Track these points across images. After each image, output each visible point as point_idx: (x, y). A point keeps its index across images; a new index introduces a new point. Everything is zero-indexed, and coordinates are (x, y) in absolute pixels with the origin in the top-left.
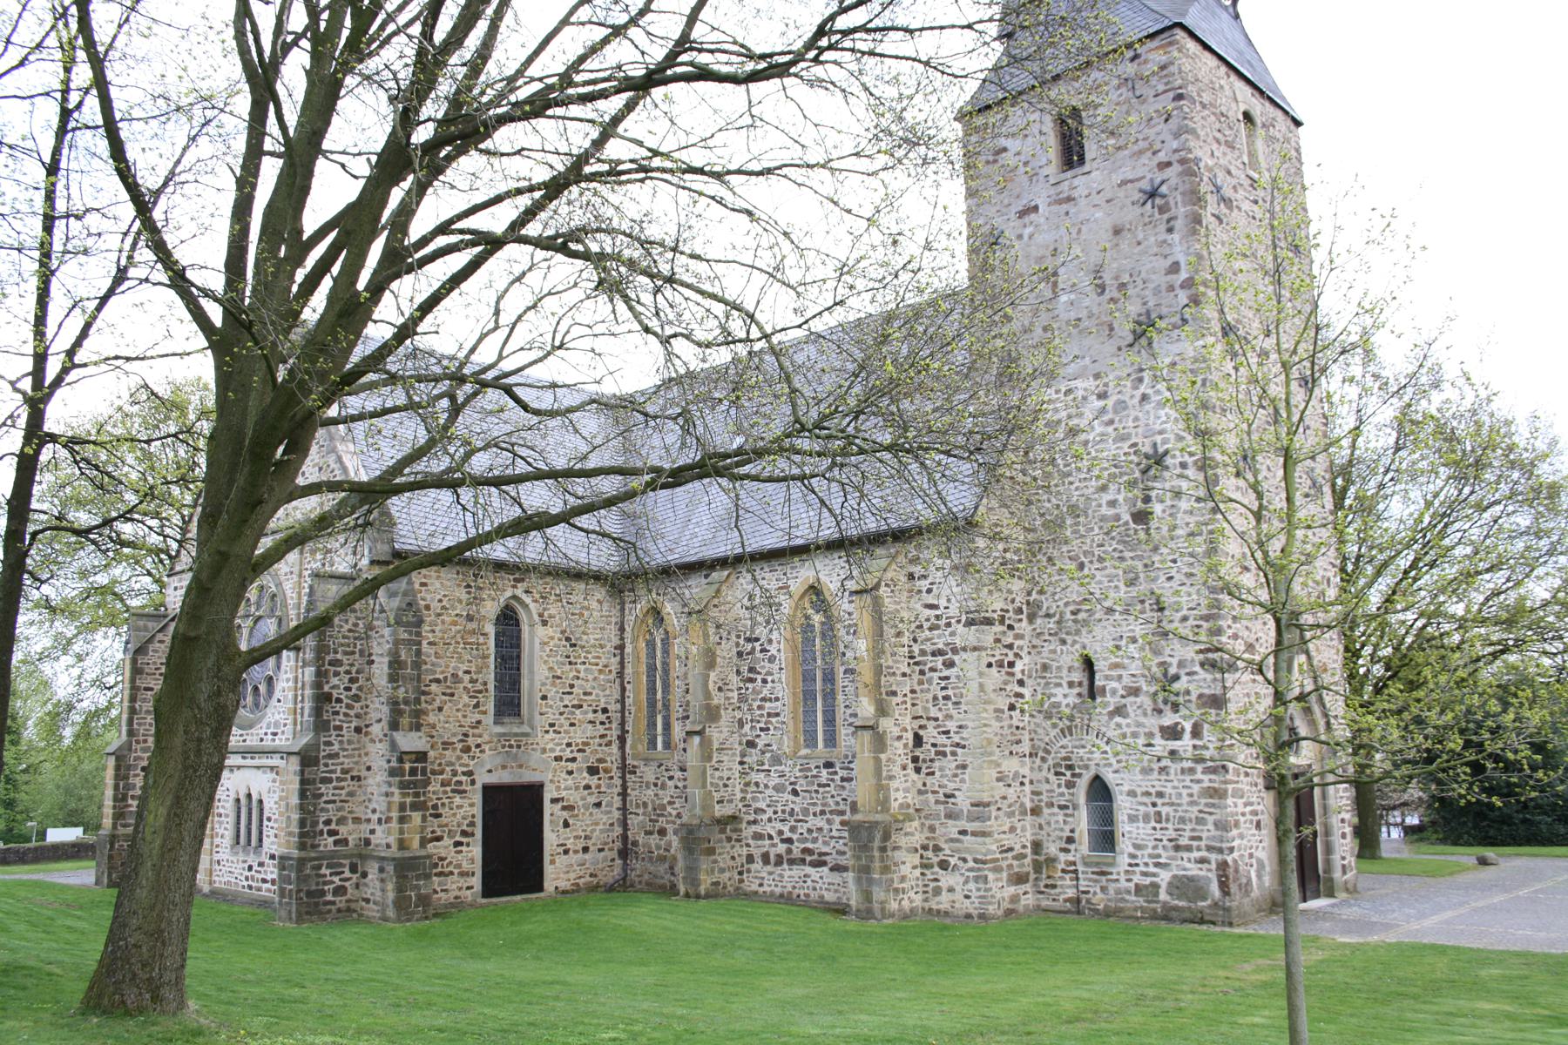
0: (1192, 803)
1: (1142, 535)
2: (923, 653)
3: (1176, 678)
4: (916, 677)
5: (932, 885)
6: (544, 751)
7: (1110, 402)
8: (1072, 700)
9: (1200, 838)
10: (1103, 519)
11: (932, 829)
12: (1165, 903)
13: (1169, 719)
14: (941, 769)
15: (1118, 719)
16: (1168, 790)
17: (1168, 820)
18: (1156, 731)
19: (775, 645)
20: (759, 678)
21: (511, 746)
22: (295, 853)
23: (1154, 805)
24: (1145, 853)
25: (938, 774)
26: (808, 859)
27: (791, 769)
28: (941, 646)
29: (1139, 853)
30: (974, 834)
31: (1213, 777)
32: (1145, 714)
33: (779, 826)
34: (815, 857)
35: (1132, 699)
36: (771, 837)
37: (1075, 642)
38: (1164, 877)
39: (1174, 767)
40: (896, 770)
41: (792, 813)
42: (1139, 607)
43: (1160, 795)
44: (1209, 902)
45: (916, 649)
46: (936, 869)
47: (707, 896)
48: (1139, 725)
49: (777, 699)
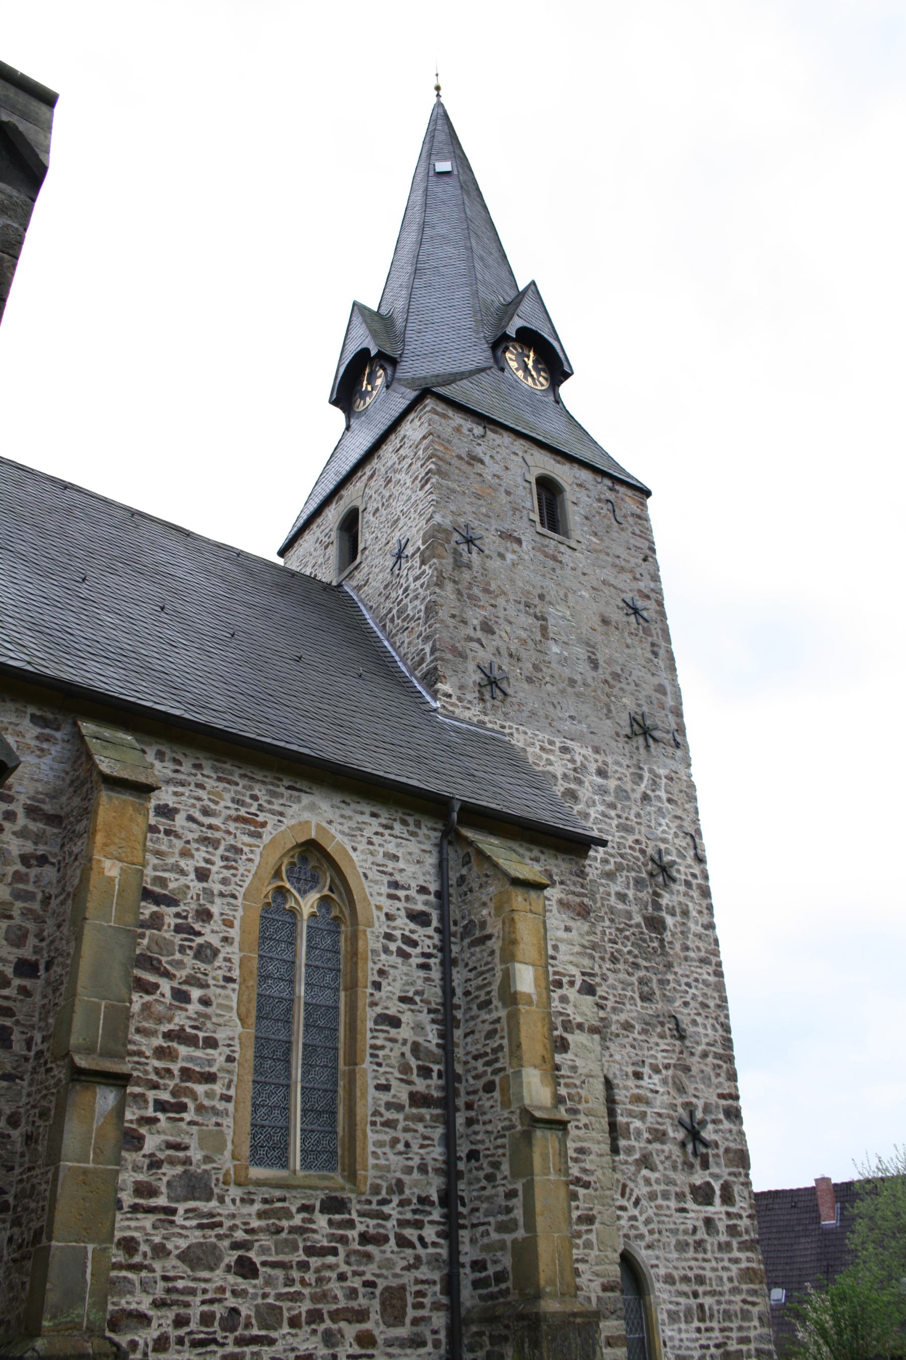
0: (735, 1291)
1: (656, 944)
3: (703, 1123)
7: (612, 784)
10: (612, 910)
13: (699, 1177)
15: (645, 1172)
16: (708, 1274)
17: (712, 1316)
18: (687, 1190)
19: (216, 923)
20: (166, 986)
23: (695, 1295)
32: (675, 1168)
39: (711, 1242)
42: (659, 1030)
48: (670, 1182)
49: (211, 1043)
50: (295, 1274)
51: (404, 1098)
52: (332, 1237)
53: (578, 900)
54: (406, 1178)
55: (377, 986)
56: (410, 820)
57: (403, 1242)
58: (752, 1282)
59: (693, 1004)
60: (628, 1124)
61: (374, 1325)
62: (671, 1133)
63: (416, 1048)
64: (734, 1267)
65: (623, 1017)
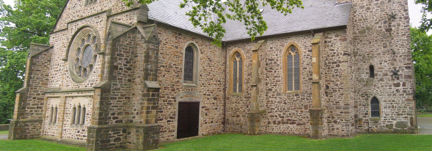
0: (403, 103)
1: (389, 35)
2: (329, 63)
3: (398, 71)
4: (327, 70)
5: (331, 128)
6: (200, 92)
8: (367, 77)
9: (405, 112)
11: (331, 112)
12: (395, 129)
13: (396, 82)
14: (335, 95)
15: (381, 82)
16: (396, 100)
18: (392, 85)
21: (189, 90)
22: (96, 126)
24: (389, 116)
25: (334, 96)
26: (289, 122)
27: (284, 97)
28: (335, 61)
29: (387, 116)
30: (345, 113)
31: (409, 96)
32: (389, 81)
33: (279, 113)
34: (292, 121)
35: (385, 77)
36: (276, 116)
37: (368, 62)
38: (394, 122)
39: (397, 94)
40: (322, 96)
41: (284, 109)
42: (388, 53)
43: (393, 101)
44: (407, 128)
45: (327, 62)
46: (333, 123)
47: (258, 135)
48: (387, 83)
50: (292, 104)
51: (308, 79)
52: (296, 99)
53: (344, 38)
54: (308, 91)
55: (303, 64)
56: (308, 35)
57: (307, 99)
58: (408, 101)
59: (399, 45)
60: (377, 74)
61: (303, 110)
62: (389, 74)
63: (309, 72)
64: (404, 99)
65: (378, 53)
